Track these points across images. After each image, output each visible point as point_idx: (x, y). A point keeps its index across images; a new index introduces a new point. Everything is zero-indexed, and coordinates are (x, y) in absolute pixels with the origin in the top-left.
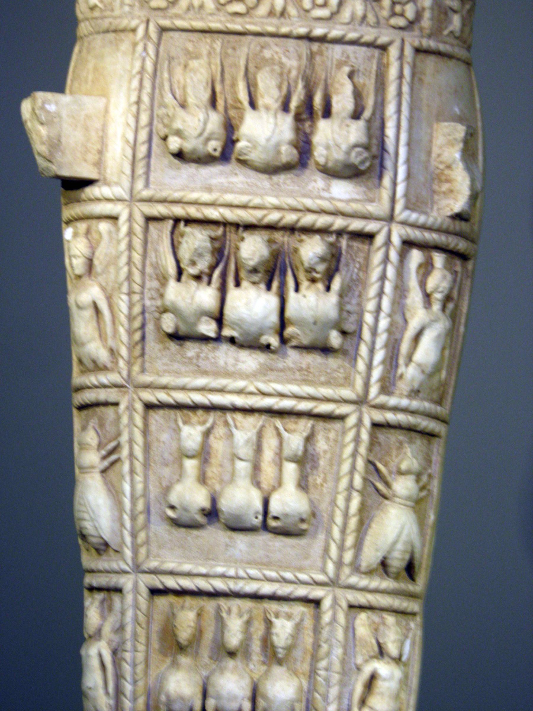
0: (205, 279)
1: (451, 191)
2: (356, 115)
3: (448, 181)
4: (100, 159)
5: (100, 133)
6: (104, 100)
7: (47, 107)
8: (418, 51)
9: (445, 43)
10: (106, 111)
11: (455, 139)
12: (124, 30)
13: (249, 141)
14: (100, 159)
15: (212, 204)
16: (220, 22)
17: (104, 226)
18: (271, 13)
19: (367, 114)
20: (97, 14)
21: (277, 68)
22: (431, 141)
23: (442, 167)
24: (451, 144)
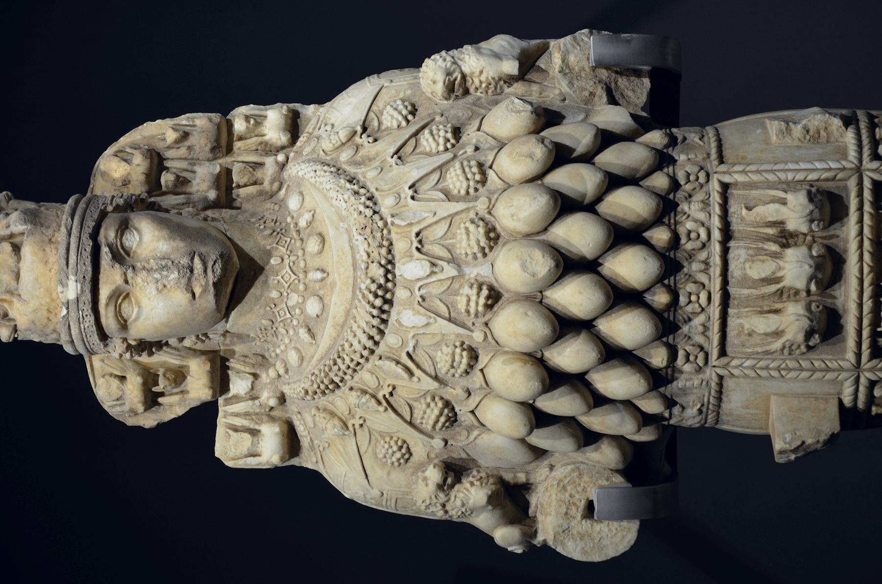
1: (826, 128)
2: (783, 202)
3: (819, 133)
5: (802, 399)
6: (773, 398)
7: (788, 440)
8: (721, 160)
9: (709, 143)
10: (783, 395)
12: (720, 385)
15: (860, 306)
16: (714, 311)
18: (706, 271)
19: (781, 194)
20: (704, 410)
21: (747, 265)
22: (789, 147)
23: (808, 137)
24: (789, 130)
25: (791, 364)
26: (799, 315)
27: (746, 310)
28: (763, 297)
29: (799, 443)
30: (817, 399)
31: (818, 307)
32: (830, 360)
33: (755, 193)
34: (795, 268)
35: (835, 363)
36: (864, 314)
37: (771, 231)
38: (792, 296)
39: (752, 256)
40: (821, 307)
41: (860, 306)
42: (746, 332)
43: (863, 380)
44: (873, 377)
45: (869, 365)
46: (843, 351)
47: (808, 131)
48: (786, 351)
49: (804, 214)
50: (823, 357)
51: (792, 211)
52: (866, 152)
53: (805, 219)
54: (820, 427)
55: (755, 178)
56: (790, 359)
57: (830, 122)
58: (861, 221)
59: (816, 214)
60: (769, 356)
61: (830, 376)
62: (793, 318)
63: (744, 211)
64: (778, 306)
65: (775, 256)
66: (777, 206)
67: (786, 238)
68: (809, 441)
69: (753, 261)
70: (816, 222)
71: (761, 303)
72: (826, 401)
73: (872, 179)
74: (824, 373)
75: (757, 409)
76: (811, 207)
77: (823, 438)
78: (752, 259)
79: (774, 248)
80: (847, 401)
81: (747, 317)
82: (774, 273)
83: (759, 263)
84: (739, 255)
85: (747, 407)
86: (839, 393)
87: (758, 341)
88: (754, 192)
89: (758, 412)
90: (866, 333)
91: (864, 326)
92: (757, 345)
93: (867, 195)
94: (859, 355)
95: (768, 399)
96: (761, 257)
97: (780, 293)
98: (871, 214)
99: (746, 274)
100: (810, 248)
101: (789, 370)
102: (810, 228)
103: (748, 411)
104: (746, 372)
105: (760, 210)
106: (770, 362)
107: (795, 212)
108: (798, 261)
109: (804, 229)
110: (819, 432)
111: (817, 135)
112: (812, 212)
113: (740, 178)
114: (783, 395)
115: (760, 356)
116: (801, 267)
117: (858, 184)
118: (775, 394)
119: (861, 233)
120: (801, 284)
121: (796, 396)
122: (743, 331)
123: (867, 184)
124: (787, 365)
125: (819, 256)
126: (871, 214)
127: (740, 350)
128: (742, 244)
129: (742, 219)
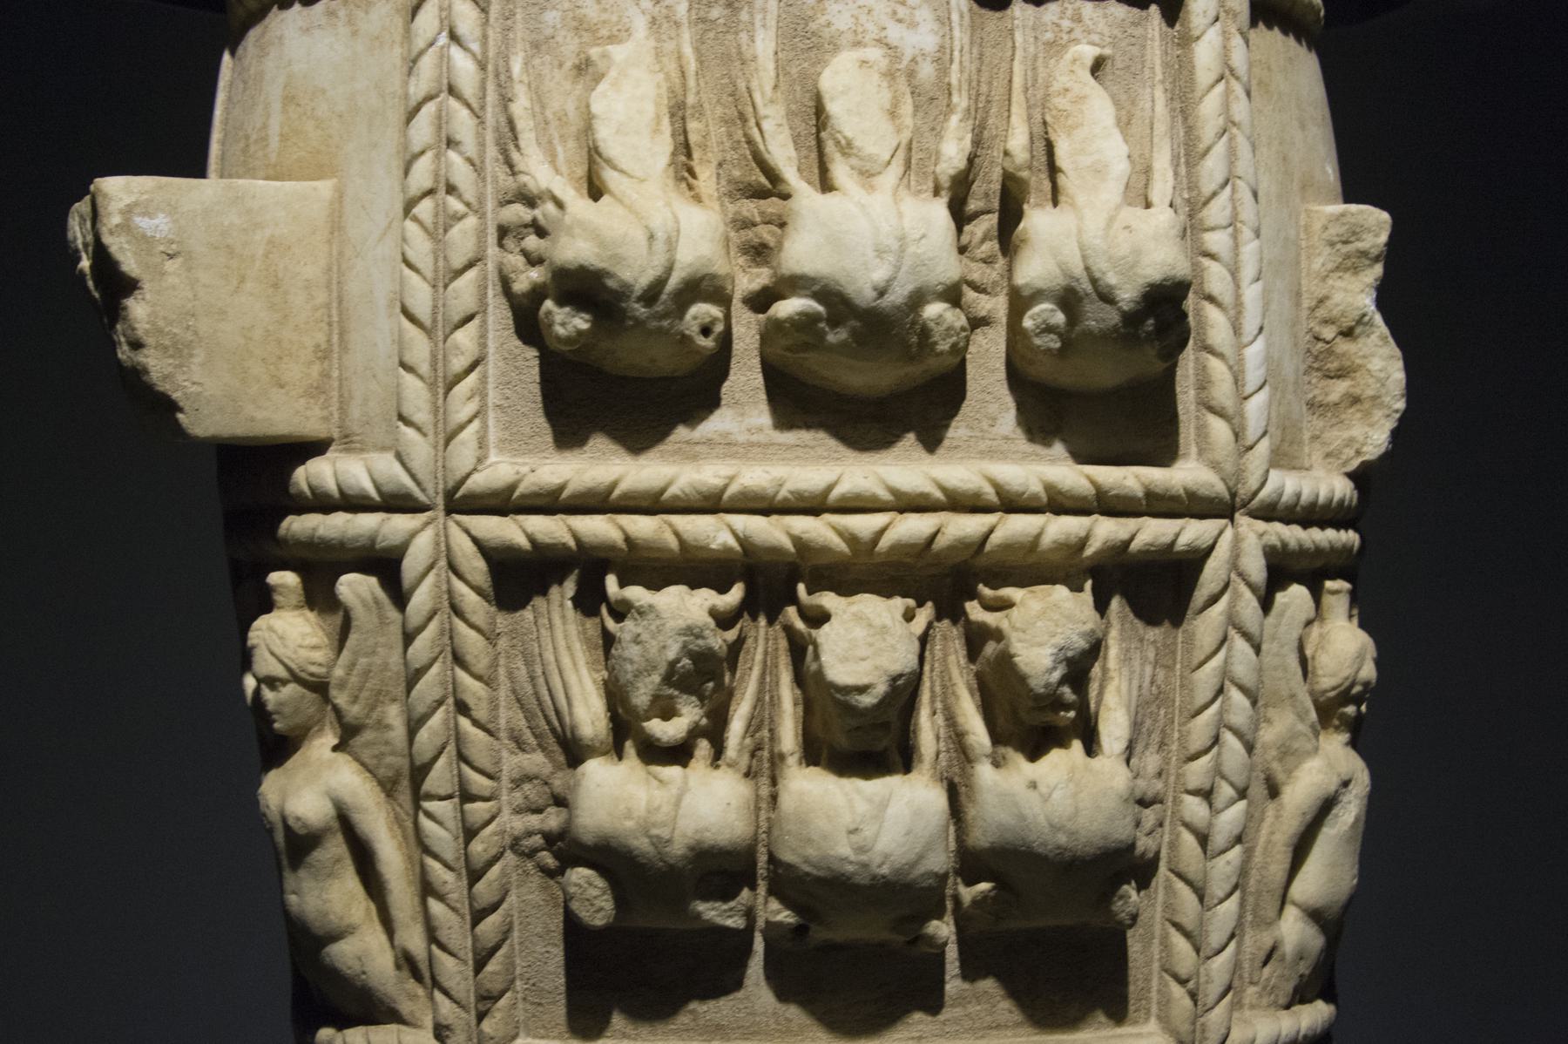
0: (703, 747)
1: (1355, 400)
3: (1341, 374)
4: (326, 375)
5: (321, 297)
6: (325, 188)
7: (143, 223)
10: (336, 224)
11: (1363, 254)
13: (816, 296)
14: (326, 375)
15: (711, 504)
17: (355, 587)
21: (874, 53)
23: (1328, 333)
24: (1351, 264)
25: (463, 239)
26: (671, 244)
27: (688, 51)
28: (742, 116)
29: (130, 264)
30: (324, 354)
31: (706, 331)
32: (480, 392)
33: (1155, 102)
34: (871, 231)
35: (472, 407)
36: (680, 521)
37: (1018, 141)
38: (749, 234)
39: (911, 74)
40: (707, 343)
41: (711, 504)
42: (594, 52)
43: (400, 524)
44: (412, 565)
45: (464, 548)
46: (515, 443)
47: (1348, 333)
48: (518, 213)
49: (1100, 265)
50: (493, 366)
51: (1111, 220)
52: (1293, 535)
53: (1078, 270)
54: (200, 355)
55: (1209, 108)
56: (481, 233)
57: (1378, 414)
58: (1058, 503)
59: (1098, 318)
60: (492, 152)
61: (416, 394)
62: (659, 219)
63: (1089, 52)
64: (707, 179)
65: (912, 159)
66: (1120, 167)
67: (993, 203)
68: (138, 309)
69: (890, 75)
70: (1059, 318)
71: (714, 112)
72: (317, 391)
73: (1212, 548)
74: (424, 368)
75: (284, 138)
76: (1127, 295)
77: (156, 364)
78: (899, 71)
79: (953, 152)
80: (318, 473)
81: (658, 54)
82: (847, 148)
83: (886, 97)
84: (913, 25)
85: (289, 99)
86: (349, 442)
87: (555, 105)
88: (1159, 94)
89: (274, 142)
90: (597, 528)
91: (627, 520)
92: (539, 99)
93: (1151, 532)
94: (503, 503)
95: (318, 173)
96: (907, 108)
97: (770, 186)
98: (1083, 543)
99: (837, 49)
100: (952, 295)
101: (438, 232)
102: (1037, 295)
103: (277, 106)
104: (427, 63)
105: (1098, 106)
106: (470, 147)
107: (1100, 229)
108: (902, 239)
109: (1034, 269)
110: (179, 350)
111: (1333, 365)
112: (1106, 297)
113: (1205, 53)
114: (336, 224)
115: (490, 115)
116: (880, 252)
117: (1192, 495)
118: (340, 195)
119: (1011, 504)
120: (803, 252)
121: (335, 277)
122: (598, 41)
123: (1192, 532)
124: (459, 218)
125: (925, 332)
126: (1083, 543)
127: (520, 31)
128: (960, 36)
129: (1055, 48)
